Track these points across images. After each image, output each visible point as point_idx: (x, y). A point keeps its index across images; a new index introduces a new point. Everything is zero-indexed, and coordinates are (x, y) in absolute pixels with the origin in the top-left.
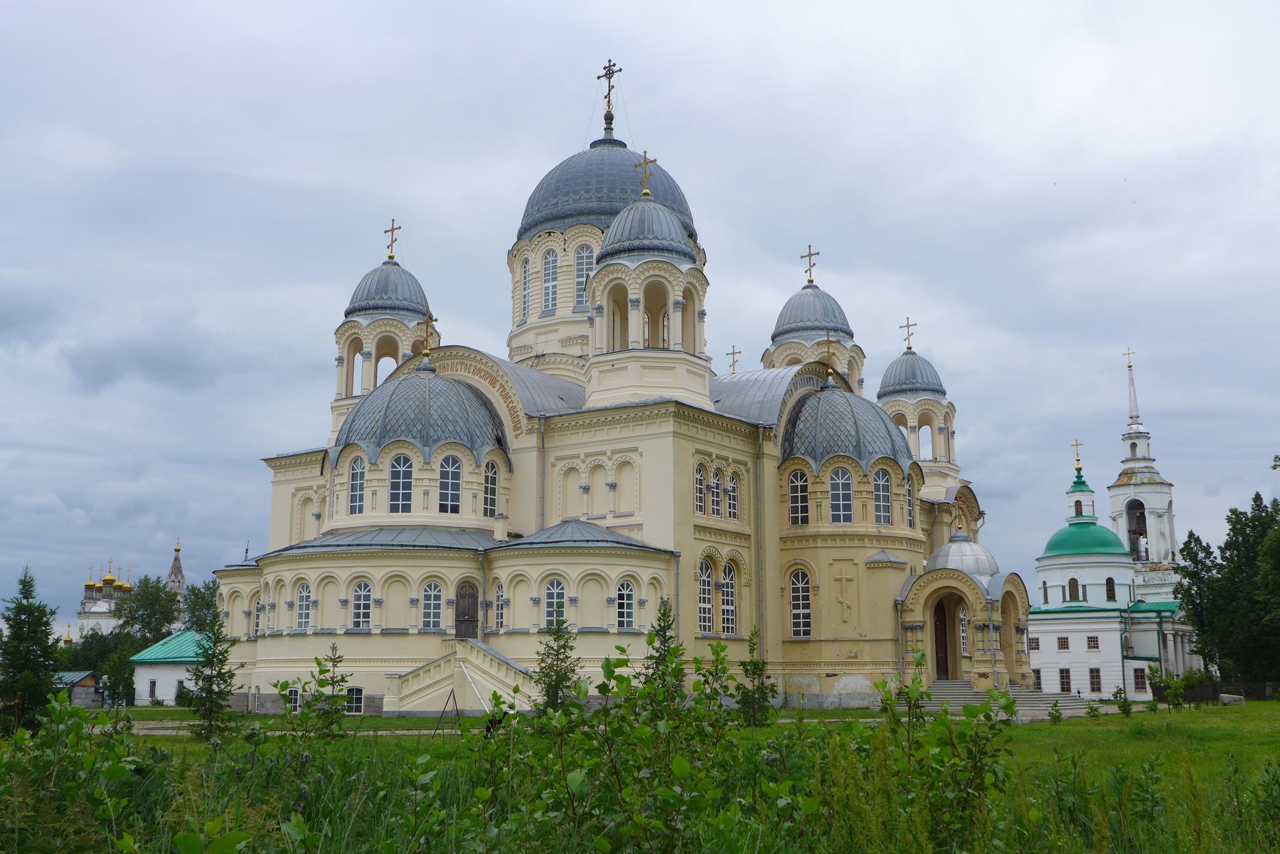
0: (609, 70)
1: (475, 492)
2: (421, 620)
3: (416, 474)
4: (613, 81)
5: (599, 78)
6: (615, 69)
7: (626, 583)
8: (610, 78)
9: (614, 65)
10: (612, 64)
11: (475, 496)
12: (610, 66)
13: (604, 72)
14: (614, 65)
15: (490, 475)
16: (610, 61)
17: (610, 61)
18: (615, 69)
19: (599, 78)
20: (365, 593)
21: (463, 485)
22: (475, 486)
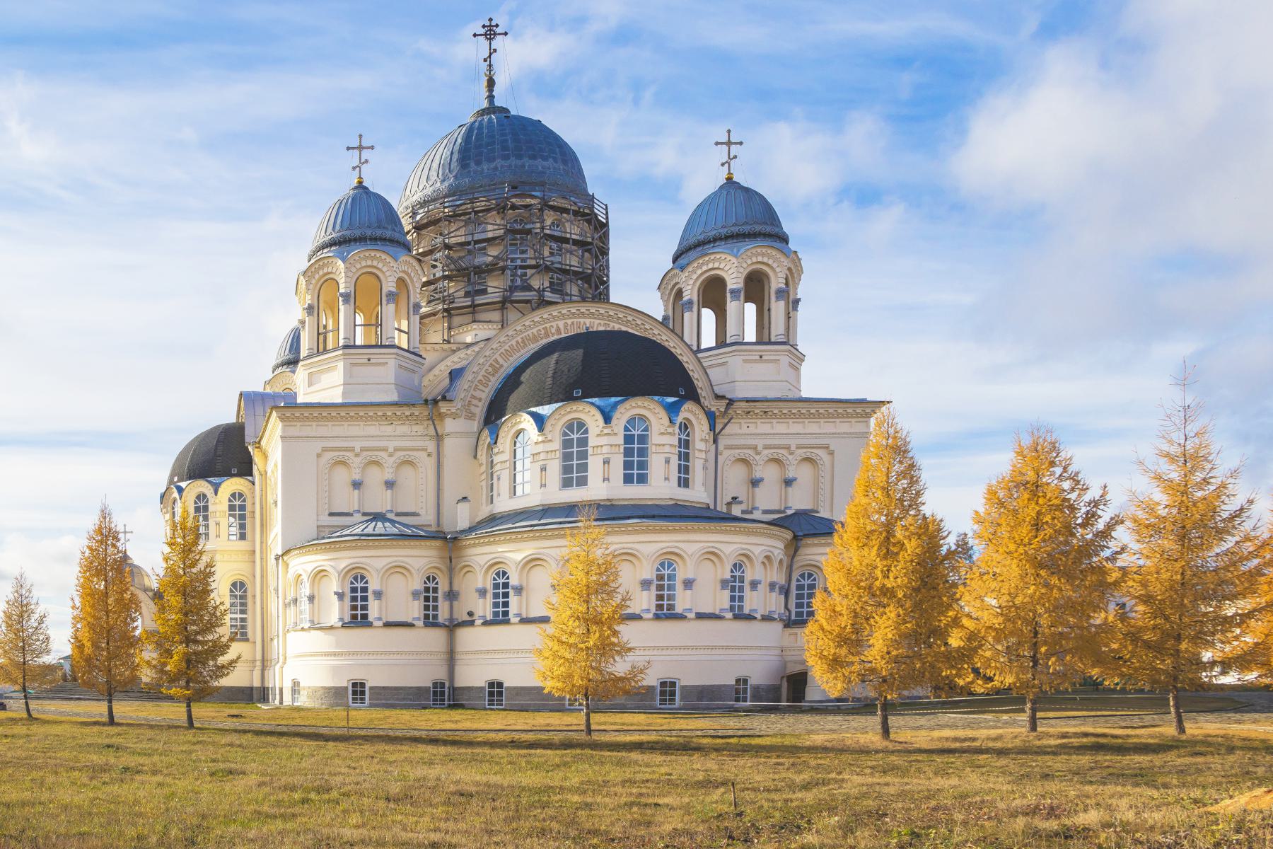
0: (490, 30)
1: (667, 455)
2: (654, 602)
3: (592, 441)
4: (498, 42)
5: (475, 35)
6: (498, 30)
7: (667, 563)
8: (490, 39)
9: (497, 26)
10: (493, 23)
11: (667, 461)
12: (490, 26)
13: (482, 31)
14: (497, 26)
15: (683, 437)
16: (491, 20)
17: (491, 20)
18: (498, 30)
19: (475, 35)
20: (503, 581)
21: (652, 449)
22: (667, 449)
